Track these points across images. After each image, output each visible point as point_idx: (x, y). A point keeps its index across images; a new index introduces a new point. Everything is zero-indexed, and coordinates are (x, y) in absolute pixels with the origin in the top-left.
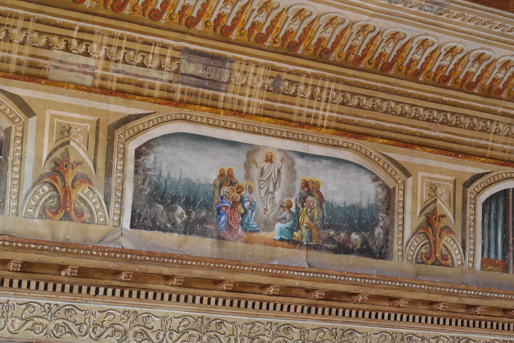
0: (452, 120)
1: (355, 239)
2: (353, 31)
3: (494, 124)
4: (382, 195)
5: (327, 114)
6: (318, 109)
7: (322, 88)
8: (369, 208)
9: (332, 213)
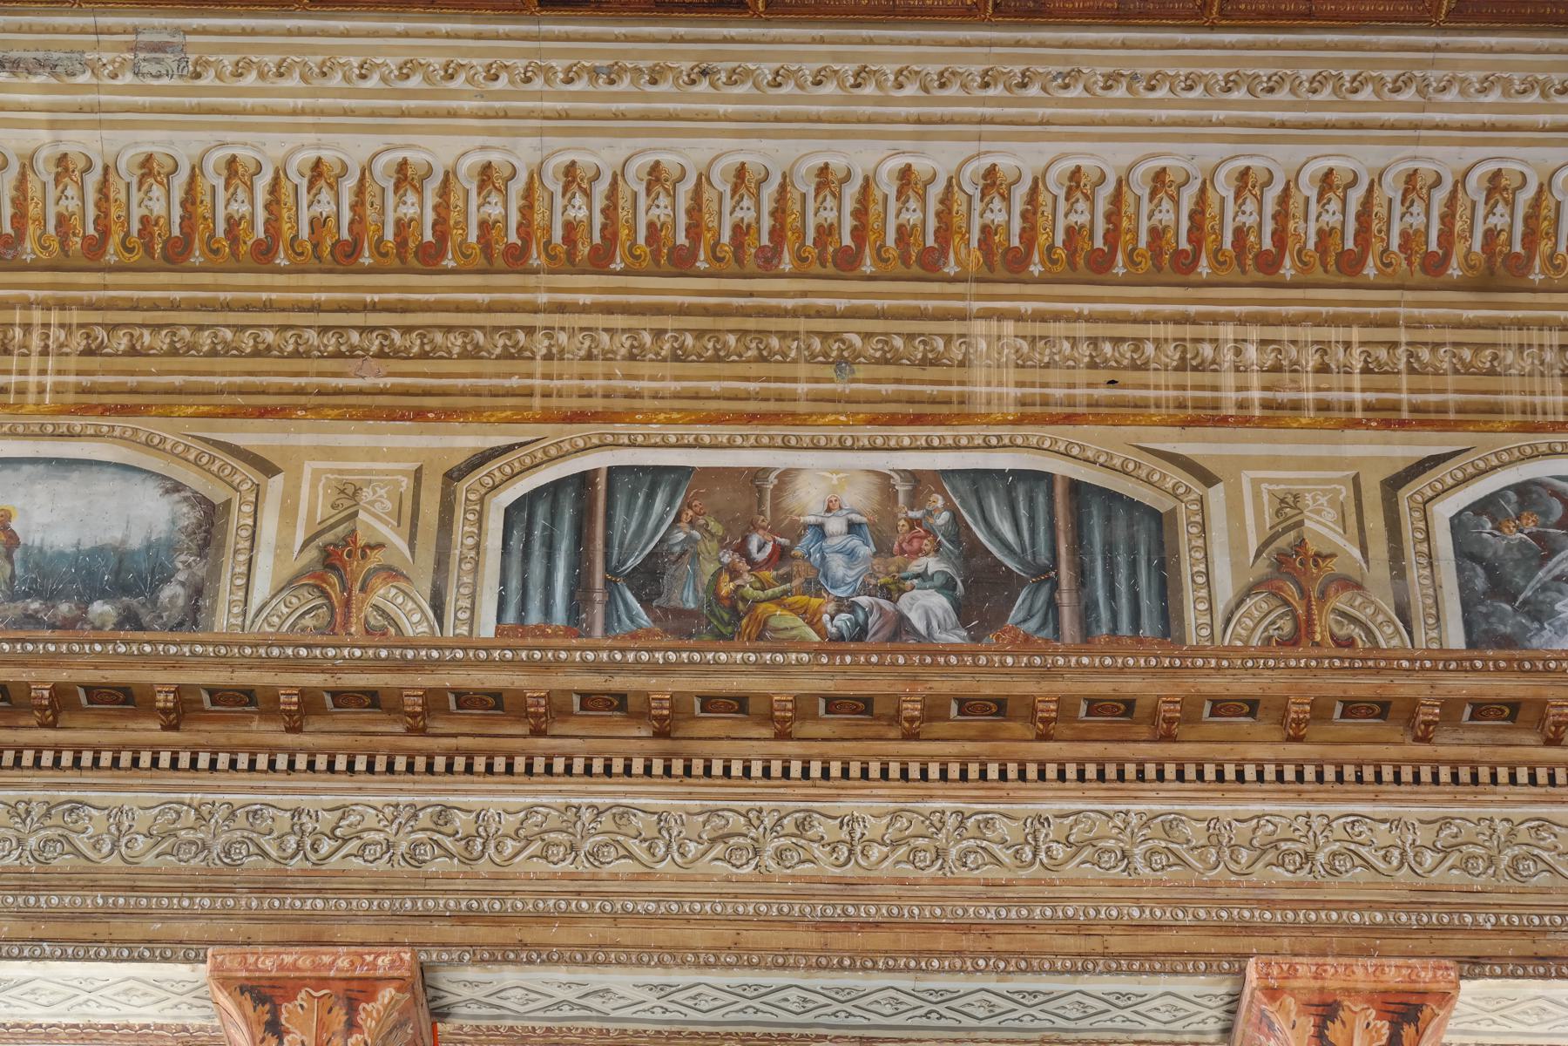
0: (408, 344)
1: (101, 614)
2: (45, 178)
3: (539, 336)
4: (189, 516)
5: (49, 380)
6: (23, 372)
7: (27, 327)
8: (149, 547)
9: (37, 565)
